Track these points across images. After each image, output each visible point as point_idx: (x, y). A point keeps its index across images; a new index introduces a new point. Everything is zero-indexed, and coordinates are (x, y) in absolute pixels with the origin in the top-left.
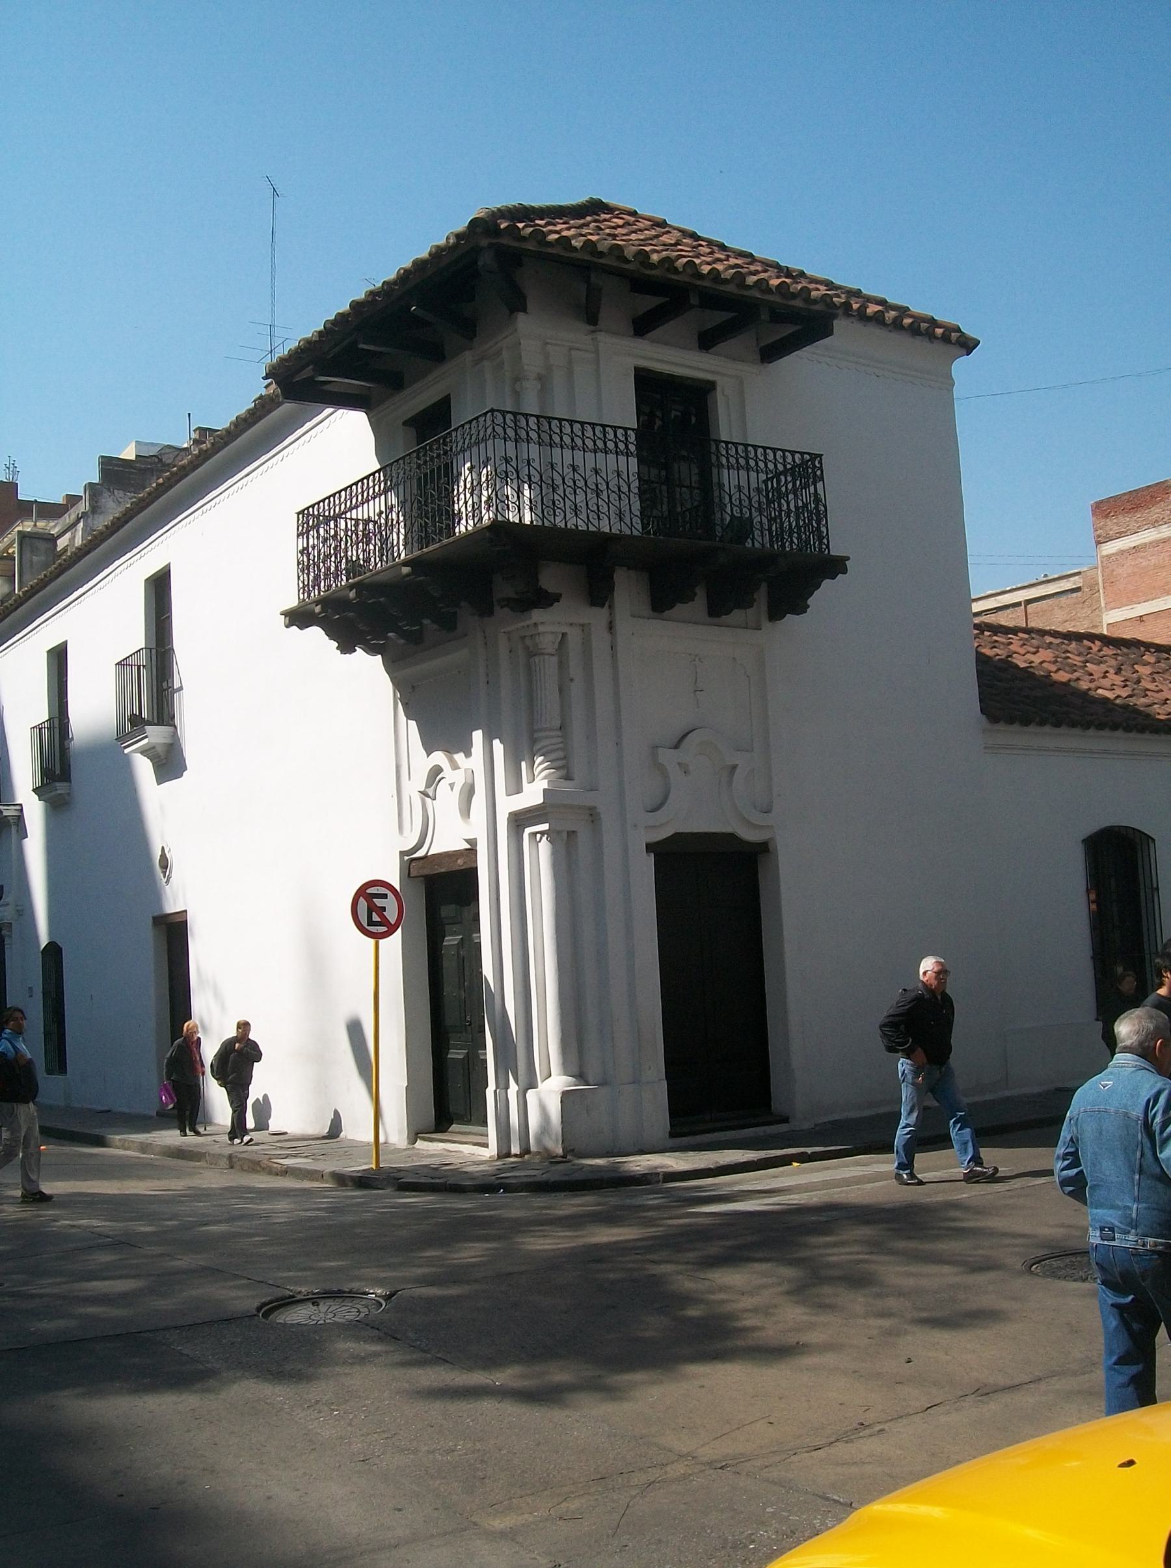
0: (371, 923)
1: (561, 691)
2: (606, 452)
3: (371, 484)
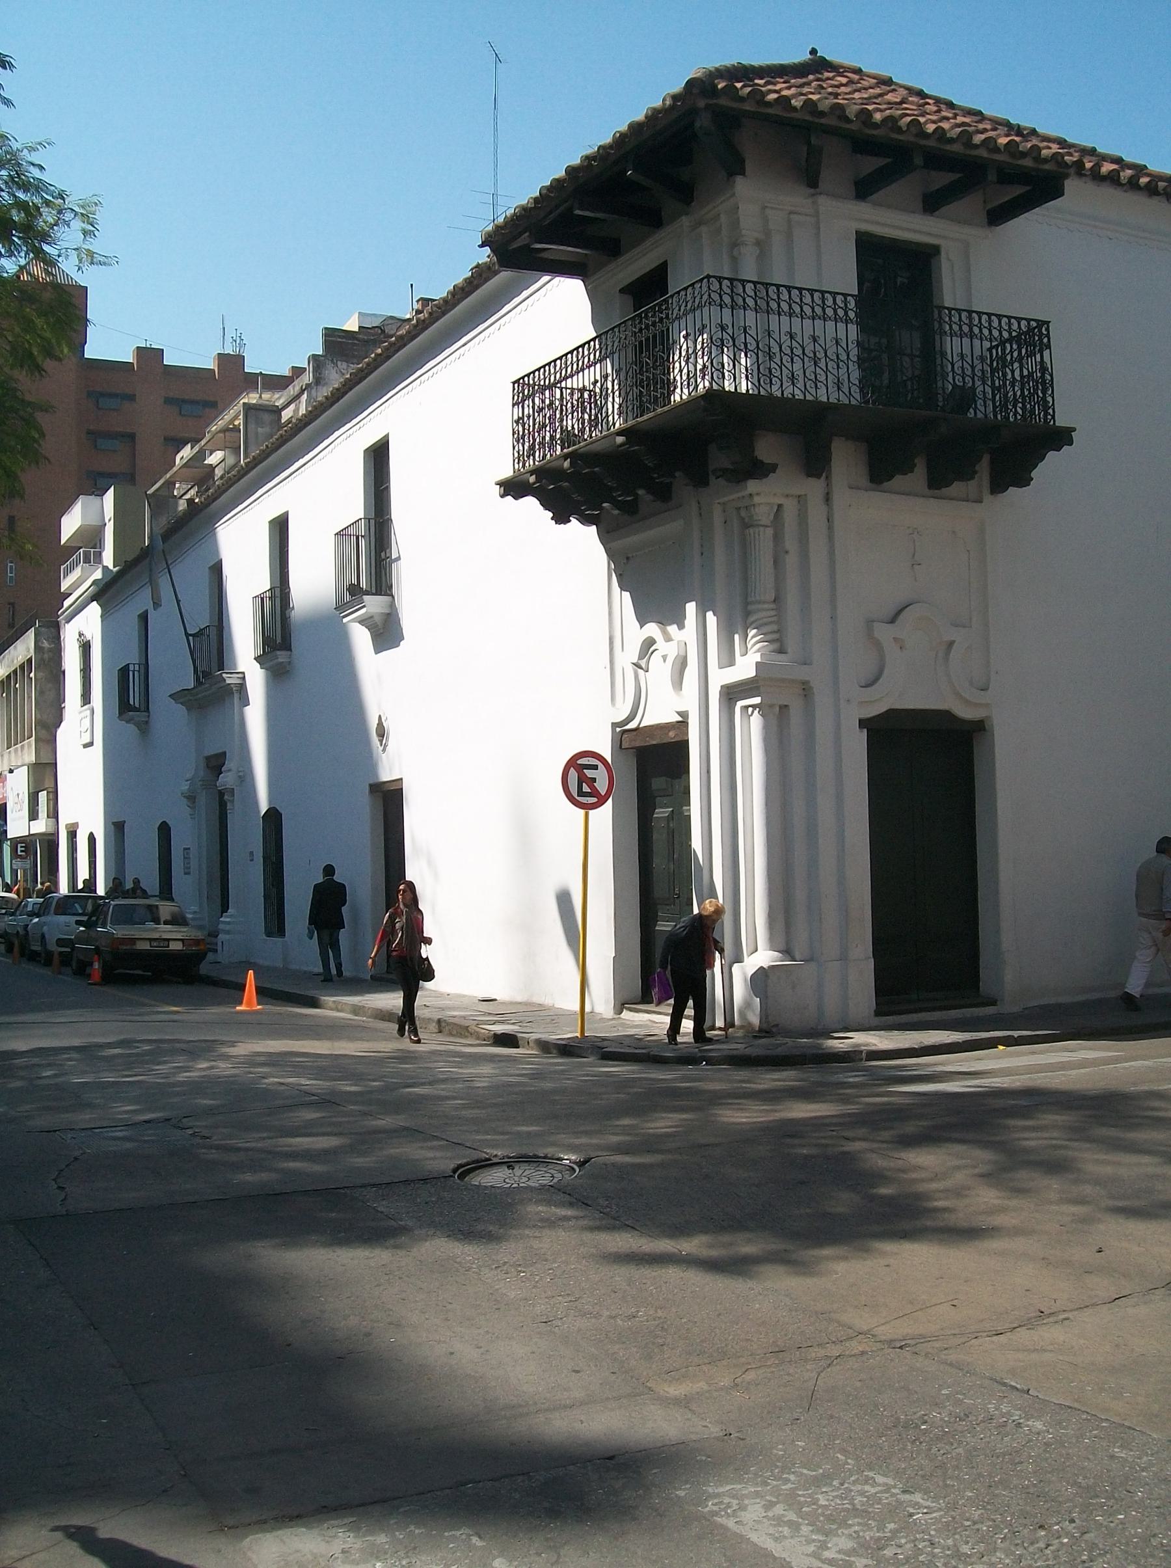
0: (581, 793)
1: (775, 562)
2: (825, 318)
3: (586, 353)
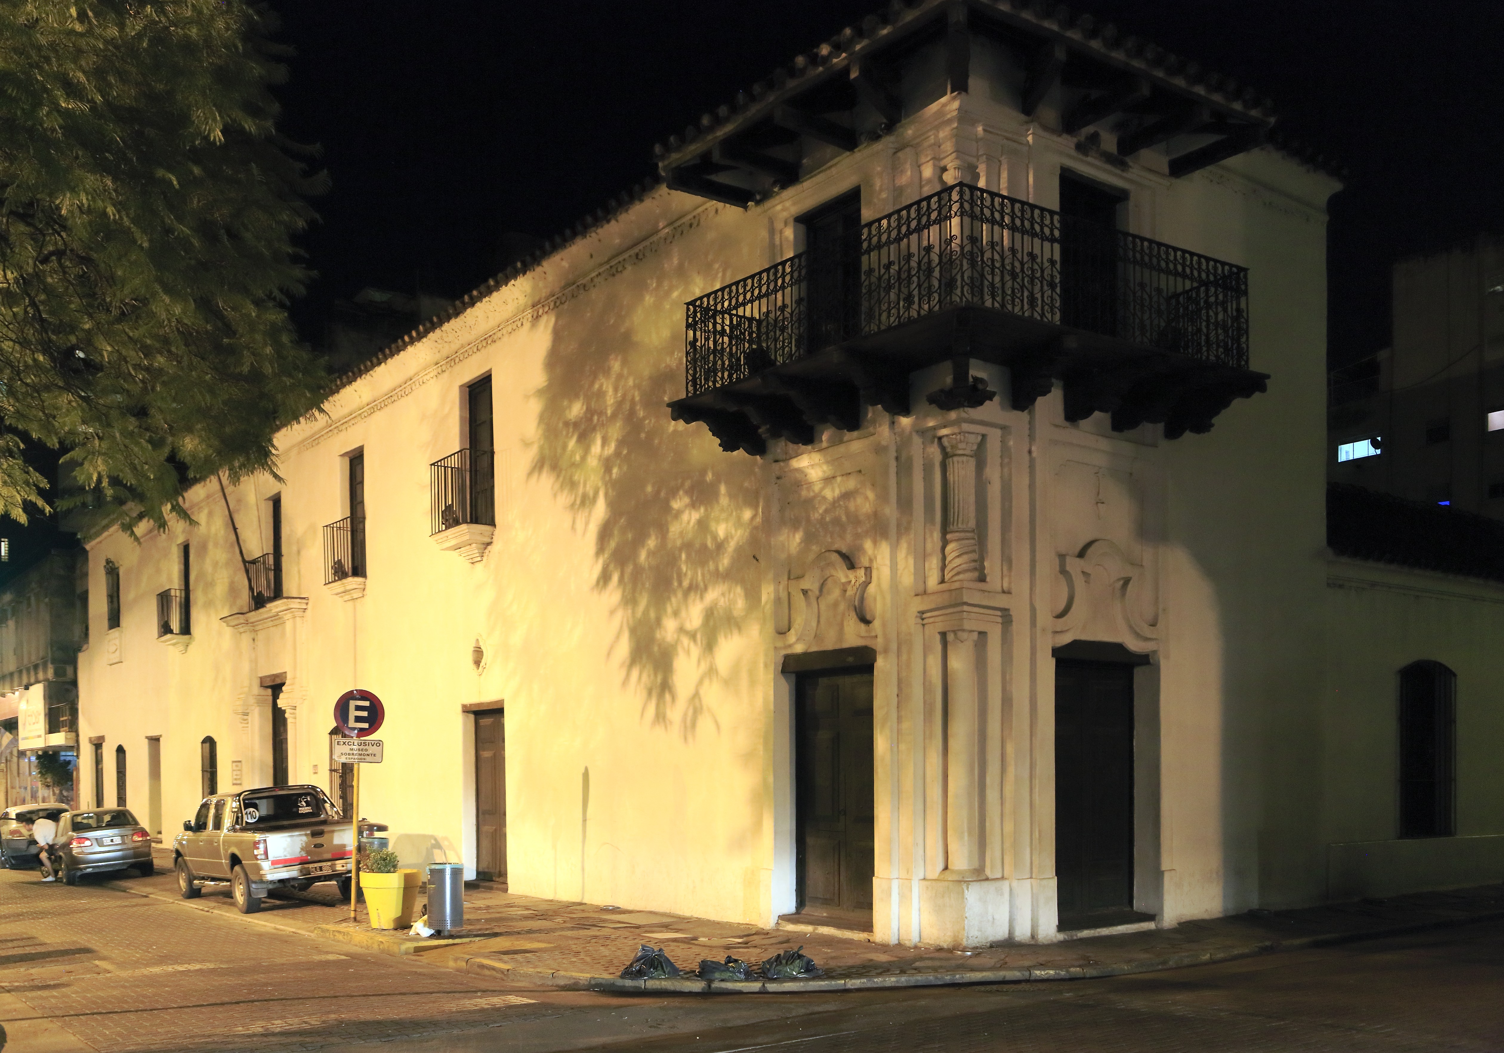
3: (741, 291)
